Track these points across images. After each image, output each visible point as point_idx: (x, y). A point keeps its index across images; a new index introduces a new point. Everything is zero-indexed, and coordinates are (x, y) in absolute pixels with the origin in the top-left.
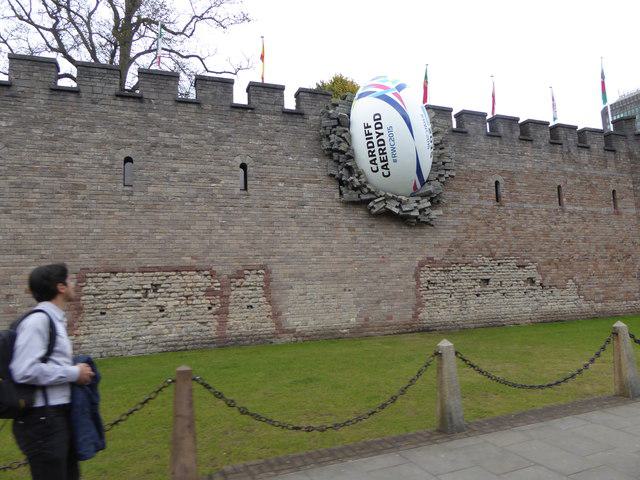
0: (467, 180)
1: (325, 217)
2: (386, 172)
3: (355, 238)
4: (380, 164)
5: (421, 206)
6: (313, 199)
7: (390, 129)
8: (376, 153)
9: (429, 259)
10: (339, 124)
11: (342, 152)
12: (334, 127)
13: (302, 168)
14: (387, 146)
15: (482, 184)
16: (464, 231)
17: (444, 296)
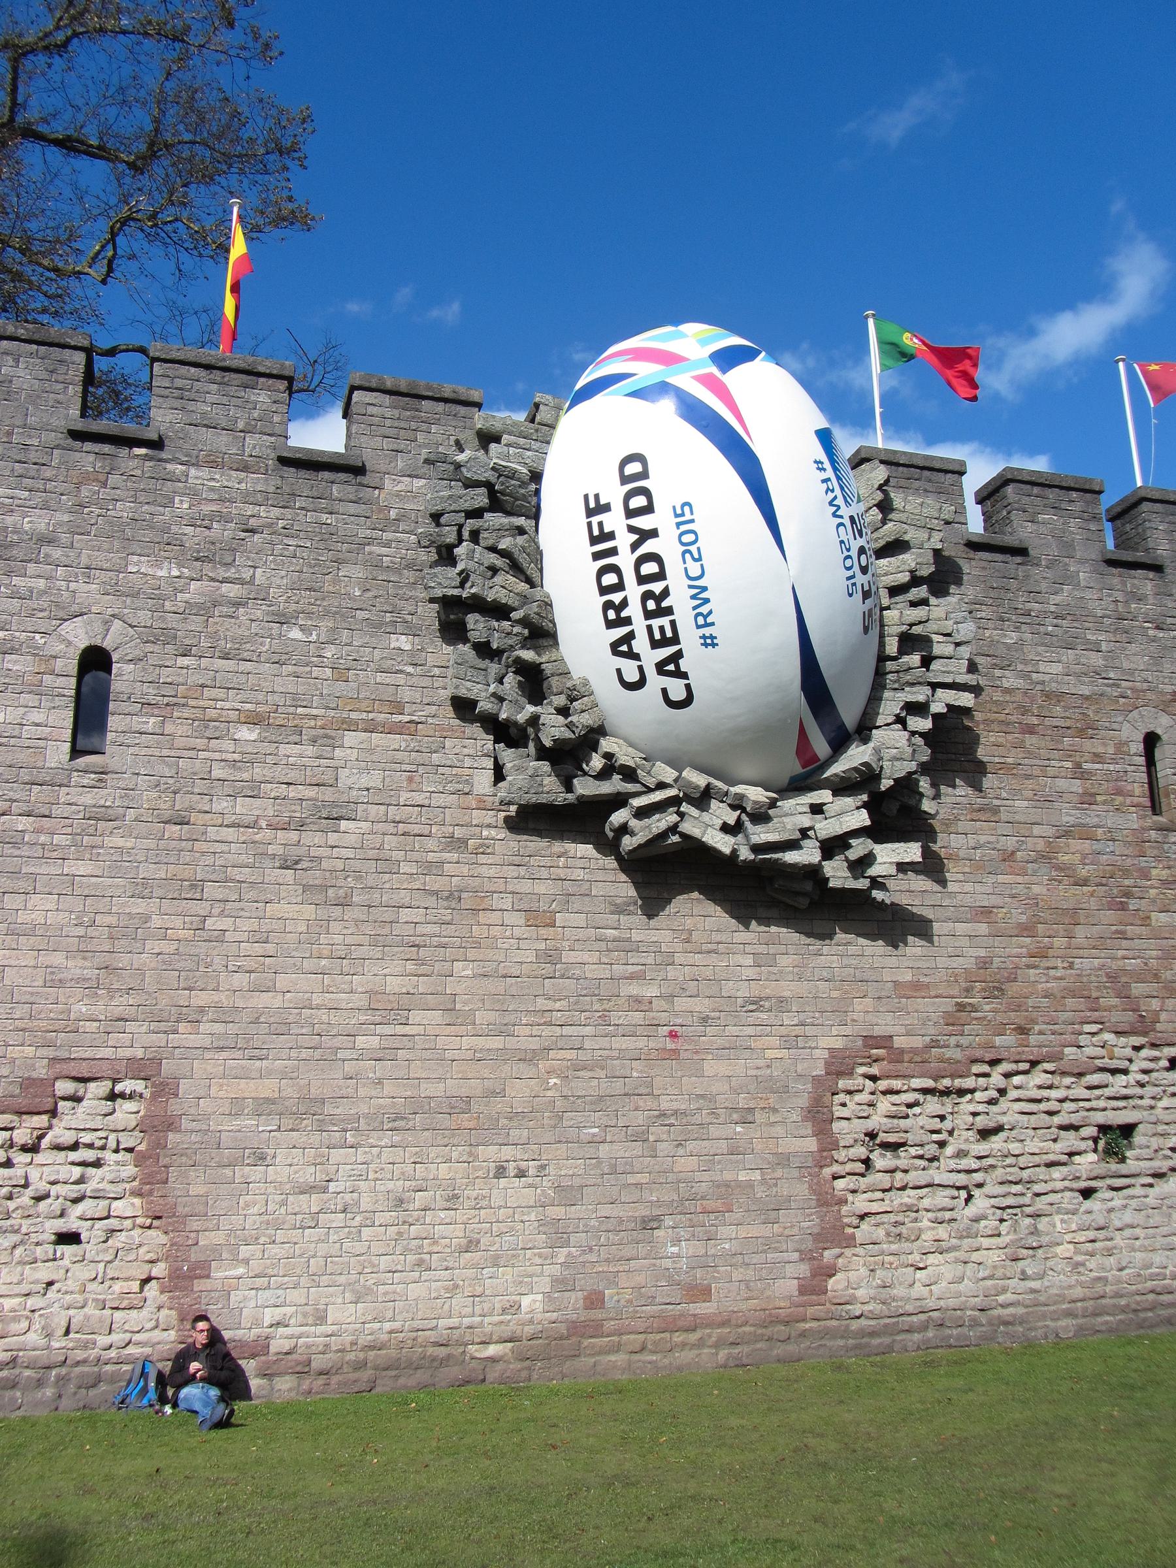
0: (1030, 730)
1: (432, 868)
2: (677, 689)
3: (550, 957)
4: (651, 657)
5: (827, 828)
6: (383, 797)
7: (683, 513)
8: (634, 610)
9: (872, 1041)
10: (496, 504)
11: (499, 611)
13: (341, 673)
15: (1088, 745)
16: (1027, 930)
17: (941, 1198)
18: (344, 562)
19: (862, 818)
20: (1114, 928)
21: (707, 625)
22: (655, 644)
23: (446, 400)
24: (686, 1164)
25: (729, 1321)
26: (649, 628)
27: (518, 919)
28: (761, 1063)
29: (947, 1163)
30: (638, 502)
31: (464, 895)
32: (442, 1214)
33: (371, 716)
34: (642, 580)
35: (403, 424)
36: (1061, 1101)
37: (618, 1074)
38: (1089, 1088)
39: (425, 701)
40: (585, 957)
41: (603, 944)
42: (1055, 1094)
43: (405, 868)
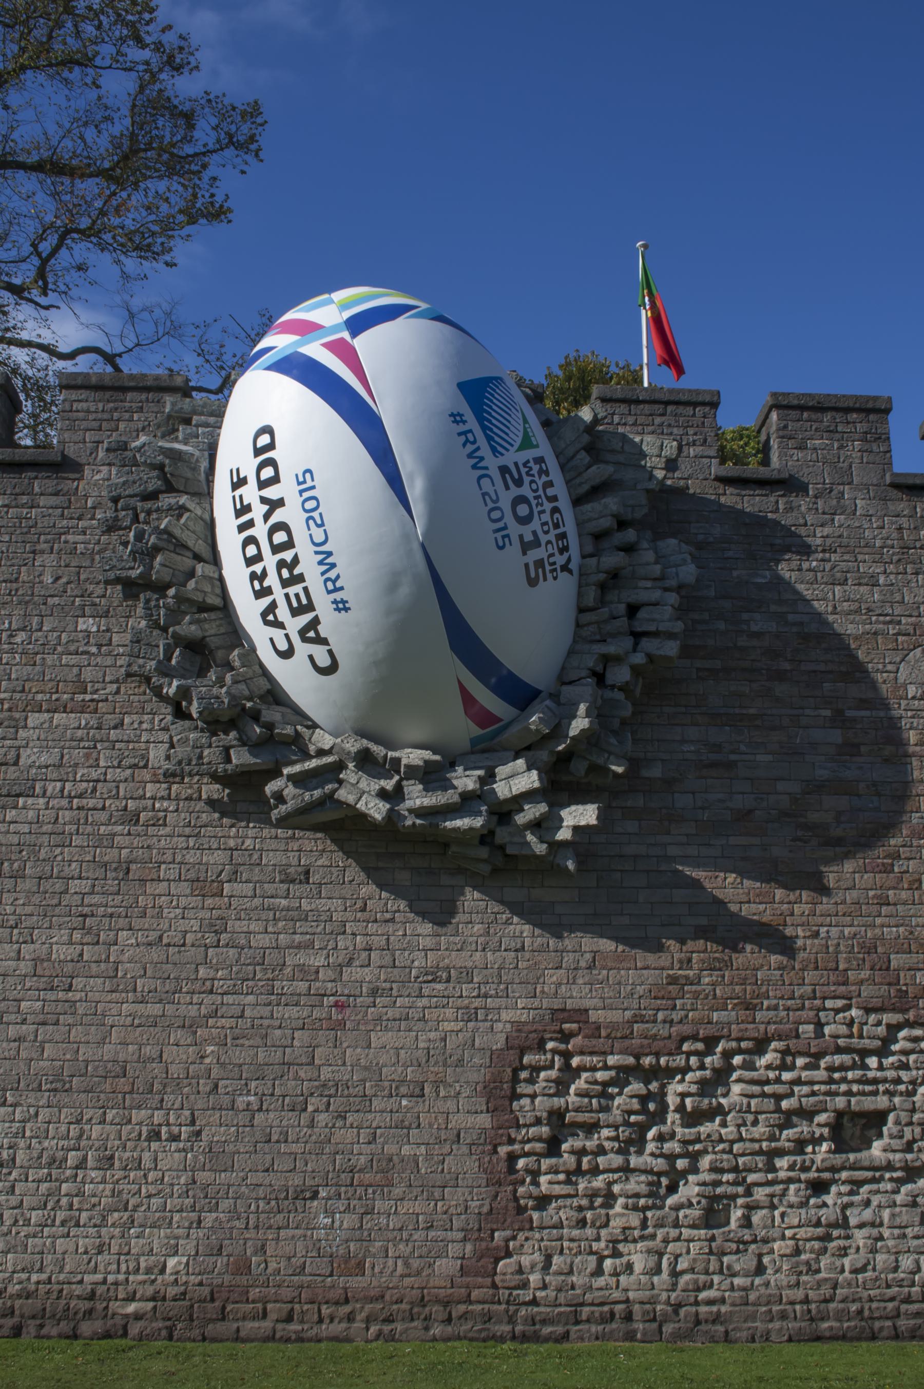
3: (217, 927)
8: (272, 580)
12: (153, 496)
14: (304, 549)
18: (42, 552)
19: (529, 780)
20: (871, 893)
21: (336, 590)
22: (295, 612)
23: (148, 389)
24: (345, 1135)
25: (383, 1297)
26: (287, 596)
27: (185, 888)
28: (432, 1035)
29: (651, 1147)
30: (268, 472)
31: (133, 867)
32: (93, 1174)
33: (54, 697)
34: (276, 549)
35: (106, 416)
36: (798, 1082)
37: (278, 1043)
38: (831, 1069)
39: (107, 679)
40: (253, 927)
41: (271, 914)
42: (786, 1076)
43: (77, 840)
